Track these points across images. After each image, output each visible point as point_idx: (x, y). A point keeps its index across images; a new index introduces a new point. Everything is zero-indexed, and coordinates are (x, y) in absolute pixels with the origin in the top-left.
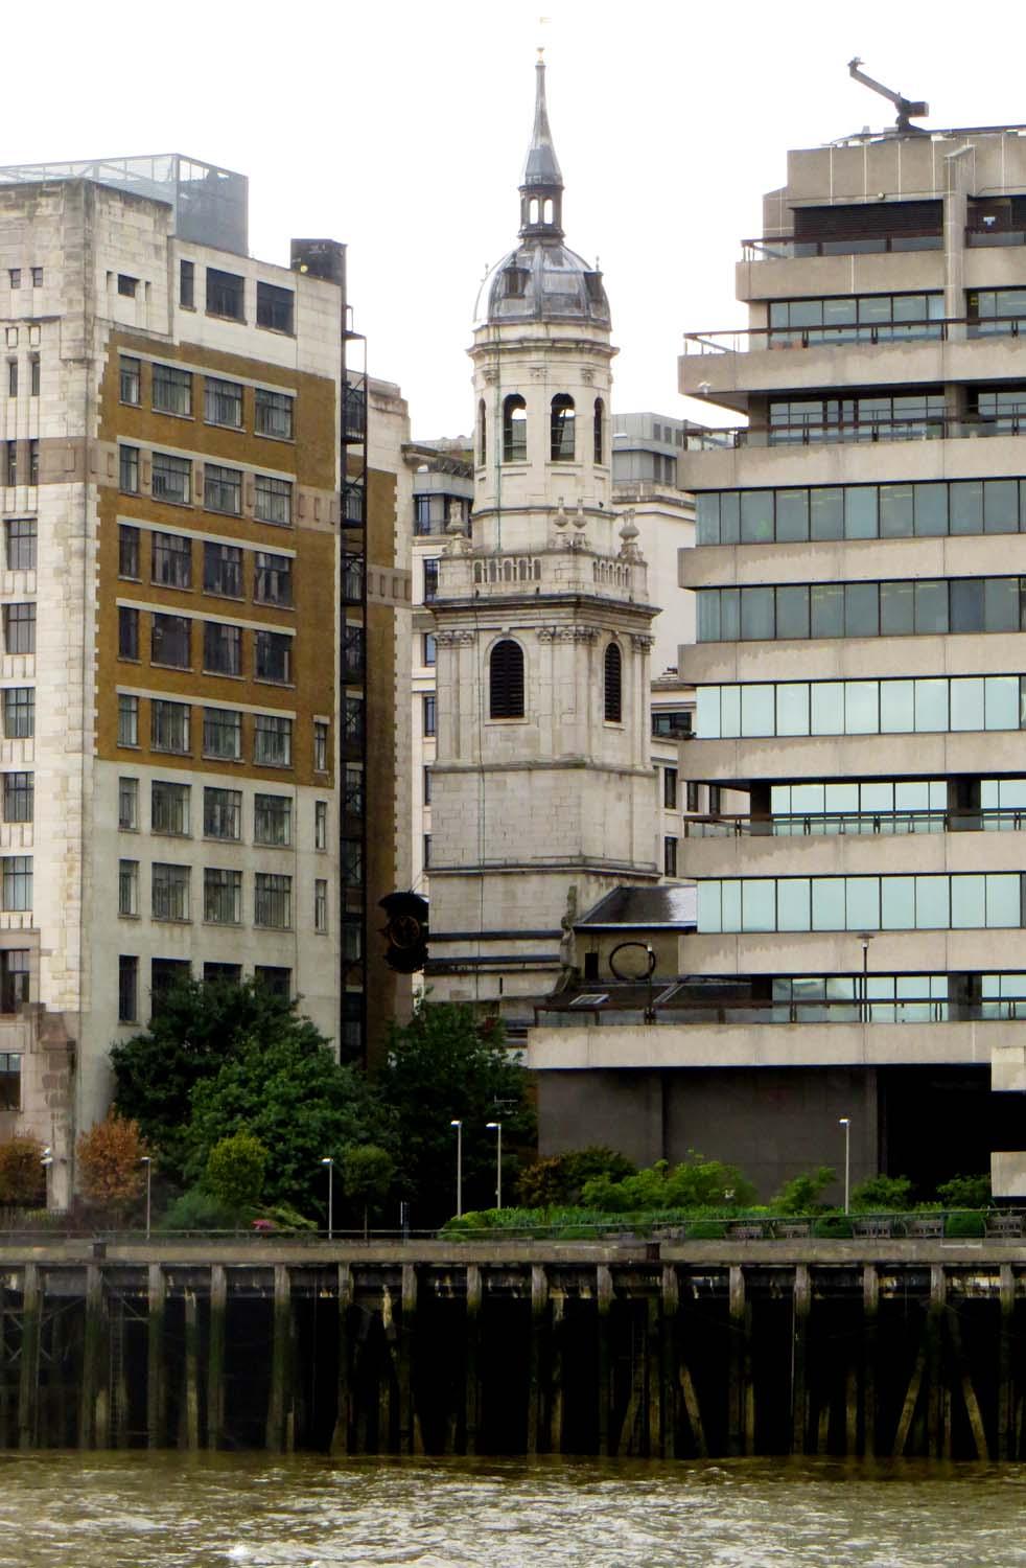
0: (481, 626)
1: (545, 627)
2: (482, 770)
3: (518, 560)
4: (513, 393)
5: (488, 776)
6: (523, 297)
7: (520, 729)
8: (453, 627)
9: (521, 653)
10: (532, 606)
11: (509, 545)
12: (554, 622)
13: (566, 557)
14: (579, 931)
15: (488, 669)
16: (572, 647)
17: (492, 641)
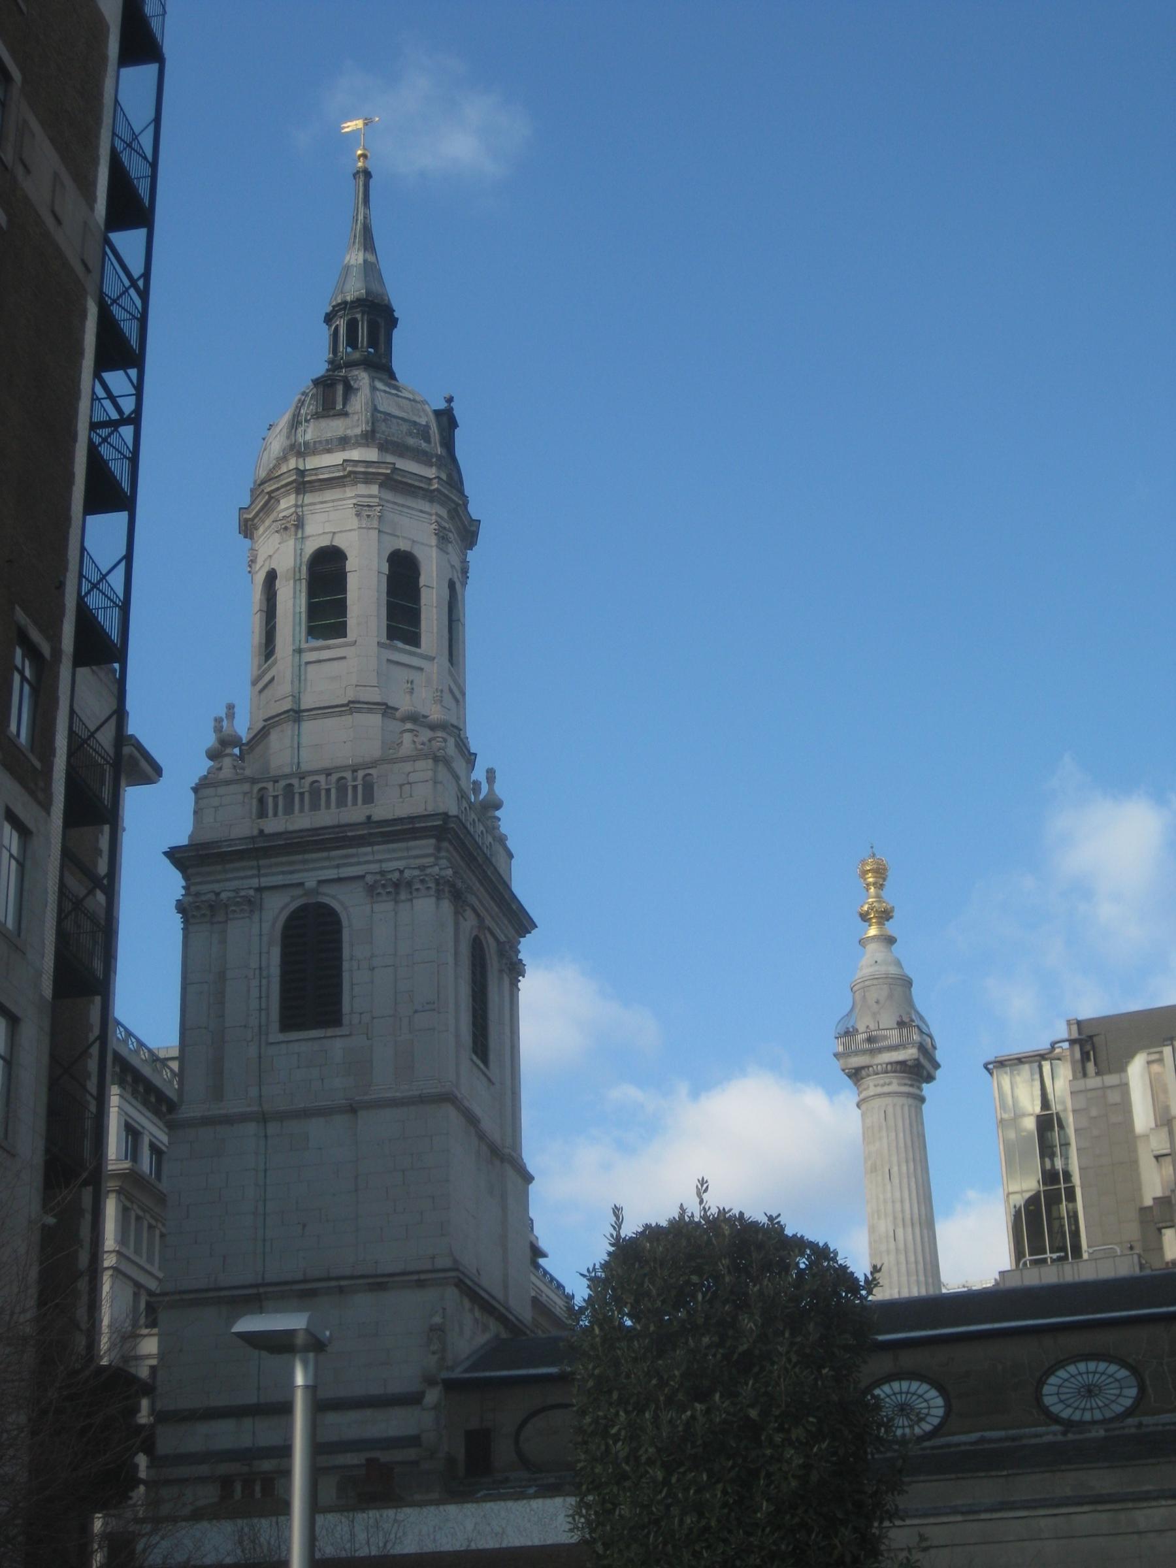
0: (266, 881)
1: (382, 873)
2: (263, 1118)
3: (334, 777)
4: (324, 542)
5: (272, 1128)
6: (345, 414)
7: (336, 1046)
8: (217, 887)
9: (338, 922)
10: (362, 841)
11: (311, 760)
12: (400, 864)
13: (421, 764)
14: (451, 1386)
15: (276, 953)
16: (433, 900)
17: (287, 905)
